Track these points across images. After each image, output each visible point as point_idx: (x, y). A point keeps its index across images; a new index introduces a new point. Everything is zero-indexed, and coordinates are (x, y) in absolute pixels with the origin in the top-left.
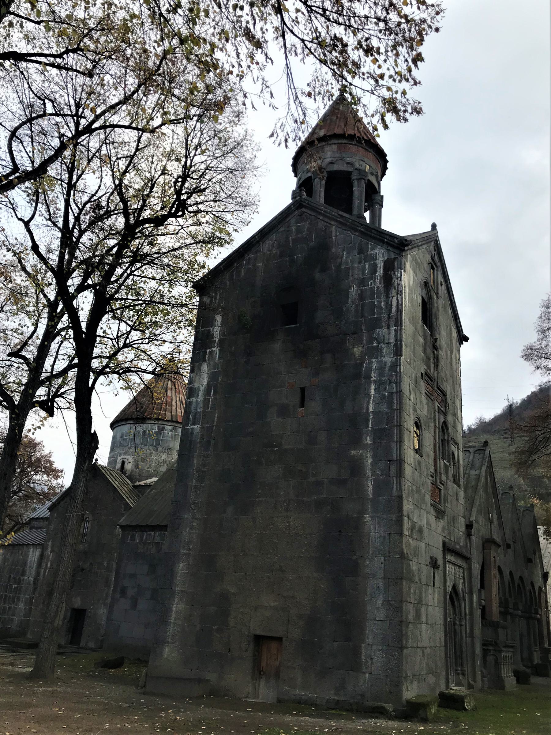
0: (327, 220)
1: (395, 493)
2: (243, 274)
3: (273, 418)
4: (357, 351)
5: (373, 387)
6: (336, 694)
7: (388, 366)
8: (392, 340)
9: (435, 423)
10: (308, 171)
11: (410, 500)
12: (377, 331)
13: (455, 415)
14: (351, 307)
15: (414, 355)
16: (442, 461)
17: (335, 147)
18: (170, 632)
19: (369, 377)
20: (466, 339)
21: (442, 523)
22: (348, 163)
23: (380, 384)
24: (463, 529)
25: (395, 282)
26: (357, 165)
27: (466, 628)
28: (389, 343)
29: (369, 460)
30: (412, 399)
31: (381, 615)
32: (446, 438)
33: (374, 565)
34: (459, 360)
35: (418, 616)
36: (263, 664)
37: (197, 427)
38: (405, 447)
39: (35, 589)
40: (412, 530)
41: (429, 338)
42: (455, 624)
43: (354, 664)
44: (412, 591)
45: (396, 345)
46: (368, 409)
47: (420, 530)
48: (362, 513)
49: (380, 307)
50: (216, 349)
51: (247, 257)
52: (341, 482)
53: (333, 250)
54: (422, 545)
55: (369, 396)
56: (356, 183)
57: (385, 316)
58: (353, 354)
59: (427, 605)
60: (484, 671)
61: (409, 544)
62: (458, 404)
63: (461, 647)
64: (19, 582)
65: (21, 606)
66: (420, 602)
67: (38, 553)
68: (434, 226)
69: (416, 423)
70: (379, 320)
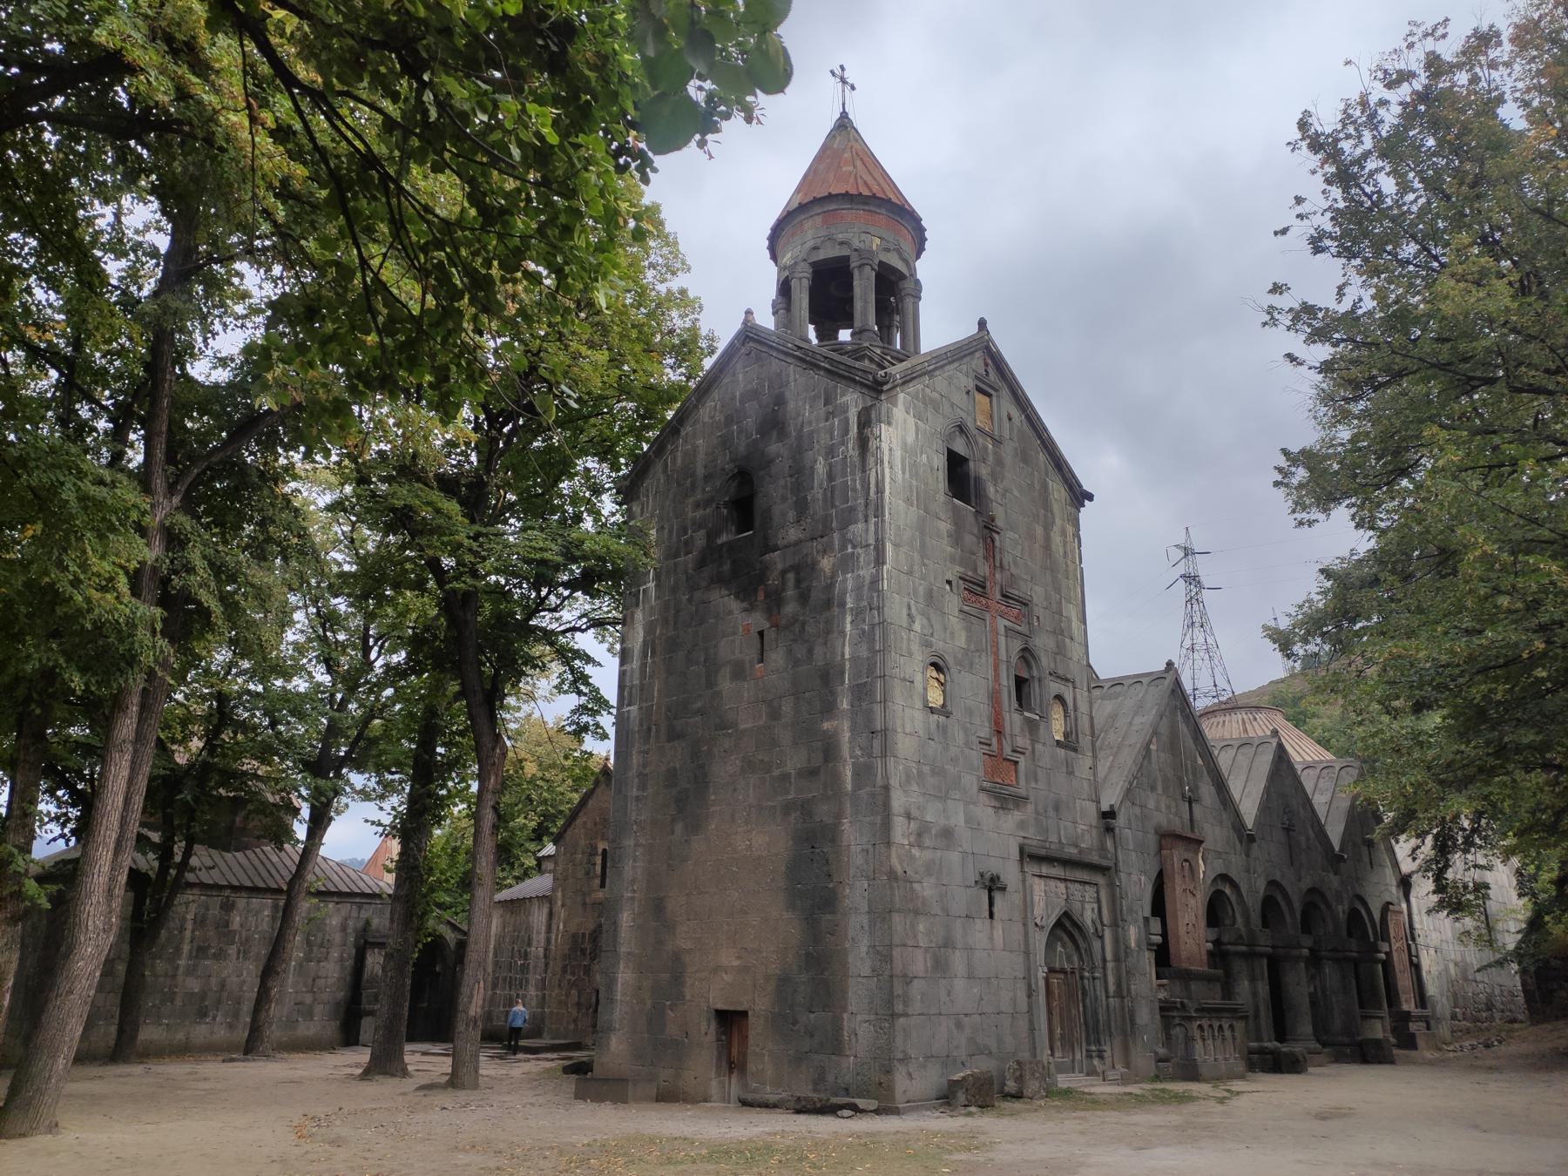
0: (782, 357)
1: (879, 781)
2: (679, 461)
3: (726, 685)
4: (826, 563)
5: (849, 619)
6: (815, 1090)
7: (867, 581)
8: (872, 541)
9: (996, 654)
10: (785, 268)
11: (915, 787)
12: (852, 528)
13: (1061, 632)
14: (817, 493)
15: (923, 555)
16: (1017, 717)
17: (819, 219)
18: (617, 1014)
19: (843, 604)
20: (1090, 497)
21: (1016, 816)
22: (842, 243)
23: (858, 614)
24: (1093, 817)
25: (873, 444)
26: (856, 243)
27: (1106, 982)
28: (868, 546)
29: (846, 736)
30: (917, 627)
31: (866, 971)
32: (1035, 673)
33: (856, 895)
34: (1077, 536)
35: (940, 966)
36: (735, 1052)
37: (634, 708)
38: (898, 708)
39: (547, 965)
40: (919, 835)
41: (971, 519)
42: (1082, 978)
43: (835, 1045)
44: (921, 927)
45: (876, 548)
46: (843, 655)
47: (947, 834)
48: (839, 816)
49: (854, 490)
50: (651, 585)
51: (683, 433)
52: (812, 773)
53: (791, 405)
54: (954, 857)
55: (843, 633)
56: (856, 273)
57: (861, 501)
58: (822, 570)
59: (969, 949)
60: (1162, 1051)
61: (912, 858)
62: (1071, 611)
63: (1095, 1013)
64: (526, 956)
65: (532, 992)
66: (948, 943)
67: (545, 911)
68: (982, 324)
69: (934, 665)
70: (852, 509)
